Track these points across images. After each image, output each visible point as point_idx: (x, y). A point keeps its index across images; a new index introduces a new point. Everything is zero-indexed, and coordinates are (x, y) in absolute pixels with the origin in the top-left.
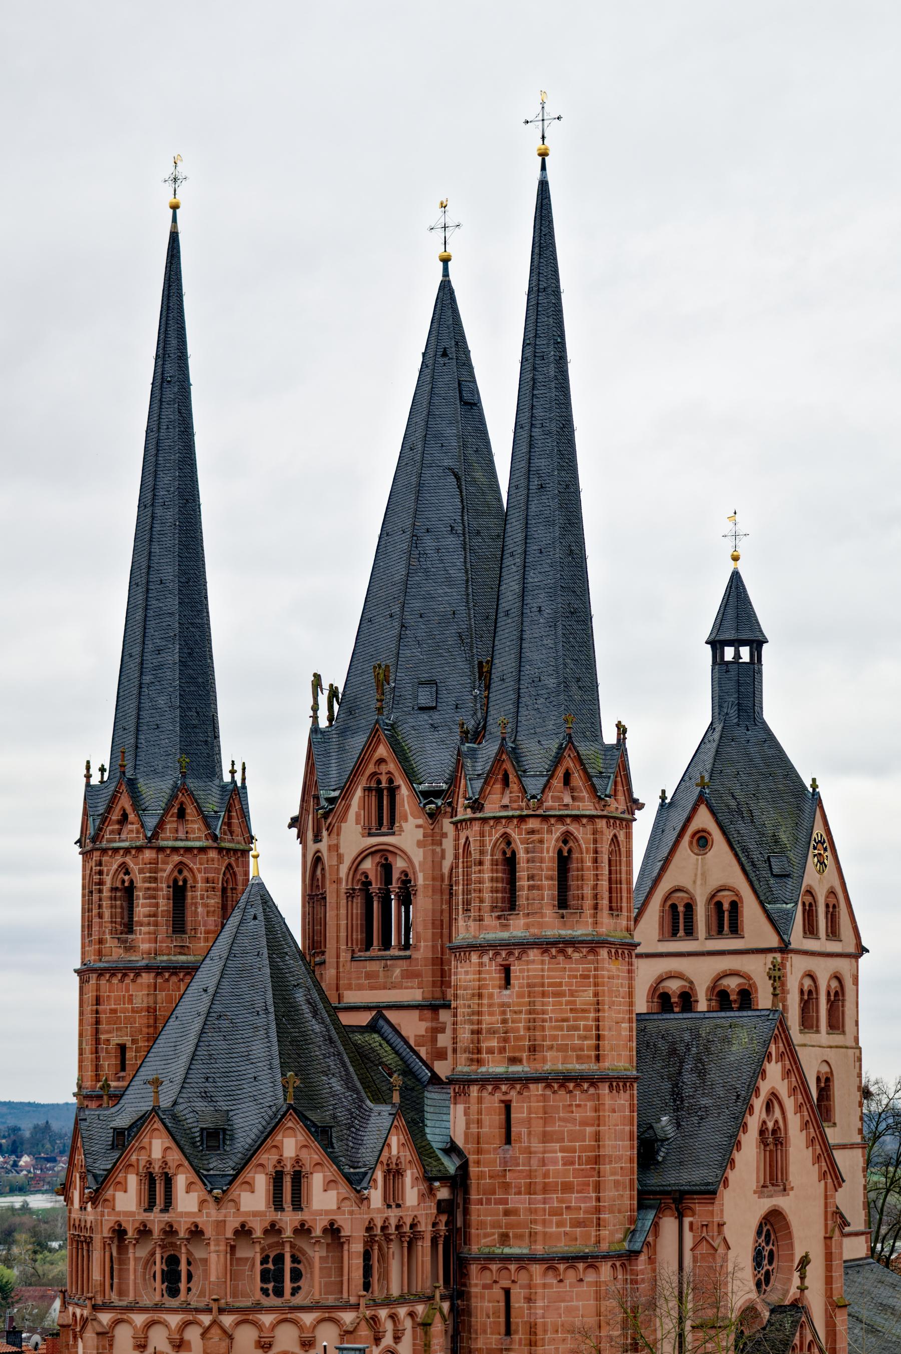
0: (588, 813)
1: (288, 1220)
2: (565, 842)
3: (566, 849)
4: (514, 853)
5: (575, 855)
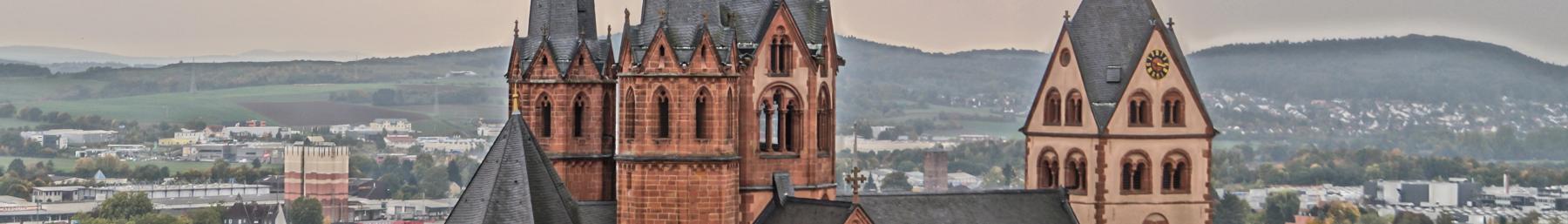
0: (673, 74)
2: (701, 94)
3: (663, 98)
4: (667, 100)
5: (707, 102)
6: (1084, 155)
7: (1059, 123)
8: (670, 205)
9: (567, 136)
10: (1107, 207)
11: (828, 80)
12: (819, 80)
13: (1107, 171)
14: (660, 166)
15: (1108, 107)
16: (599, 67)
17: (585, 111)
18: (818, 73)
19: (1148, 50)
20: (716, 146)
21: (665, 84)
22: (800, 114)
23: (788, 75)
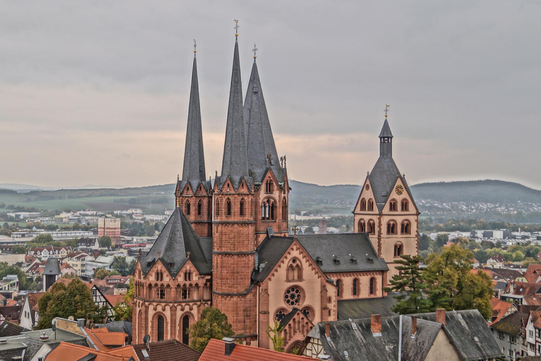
1: (188, 283)
2: (242, 200)
3: (229, 201)
4: (230, 202)
5: (244, 203)
6: (374, 221)
7: (365, 210)
8: (231, 239)
9: (196, 215)
10: (382, 239)
11: (286, 195)
12: (283, 195)
13: (382, 227)
14: (228, 225)
15: (382, 205)
16: (207, 191)
17: (202, 206)
18: (282, 193)
19: (396, 185)
20: (247, 218)
21: (229, 197)
22: (276, 207)
23: (272, 194)
